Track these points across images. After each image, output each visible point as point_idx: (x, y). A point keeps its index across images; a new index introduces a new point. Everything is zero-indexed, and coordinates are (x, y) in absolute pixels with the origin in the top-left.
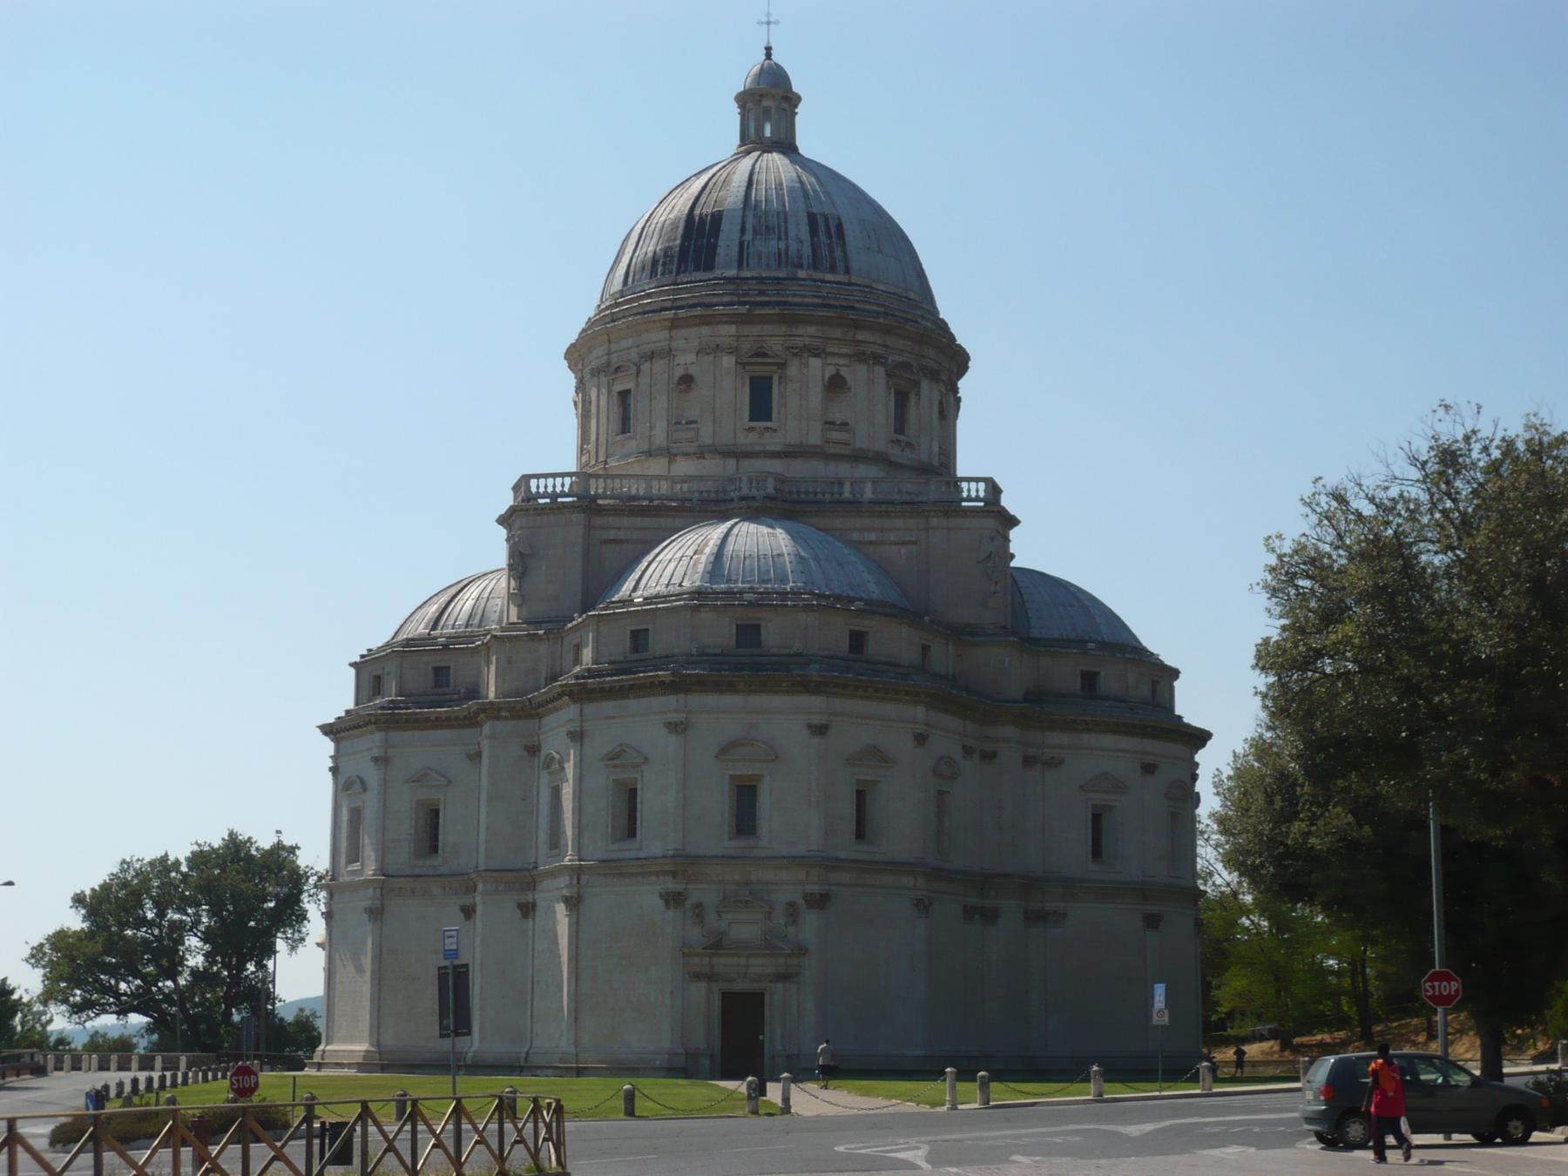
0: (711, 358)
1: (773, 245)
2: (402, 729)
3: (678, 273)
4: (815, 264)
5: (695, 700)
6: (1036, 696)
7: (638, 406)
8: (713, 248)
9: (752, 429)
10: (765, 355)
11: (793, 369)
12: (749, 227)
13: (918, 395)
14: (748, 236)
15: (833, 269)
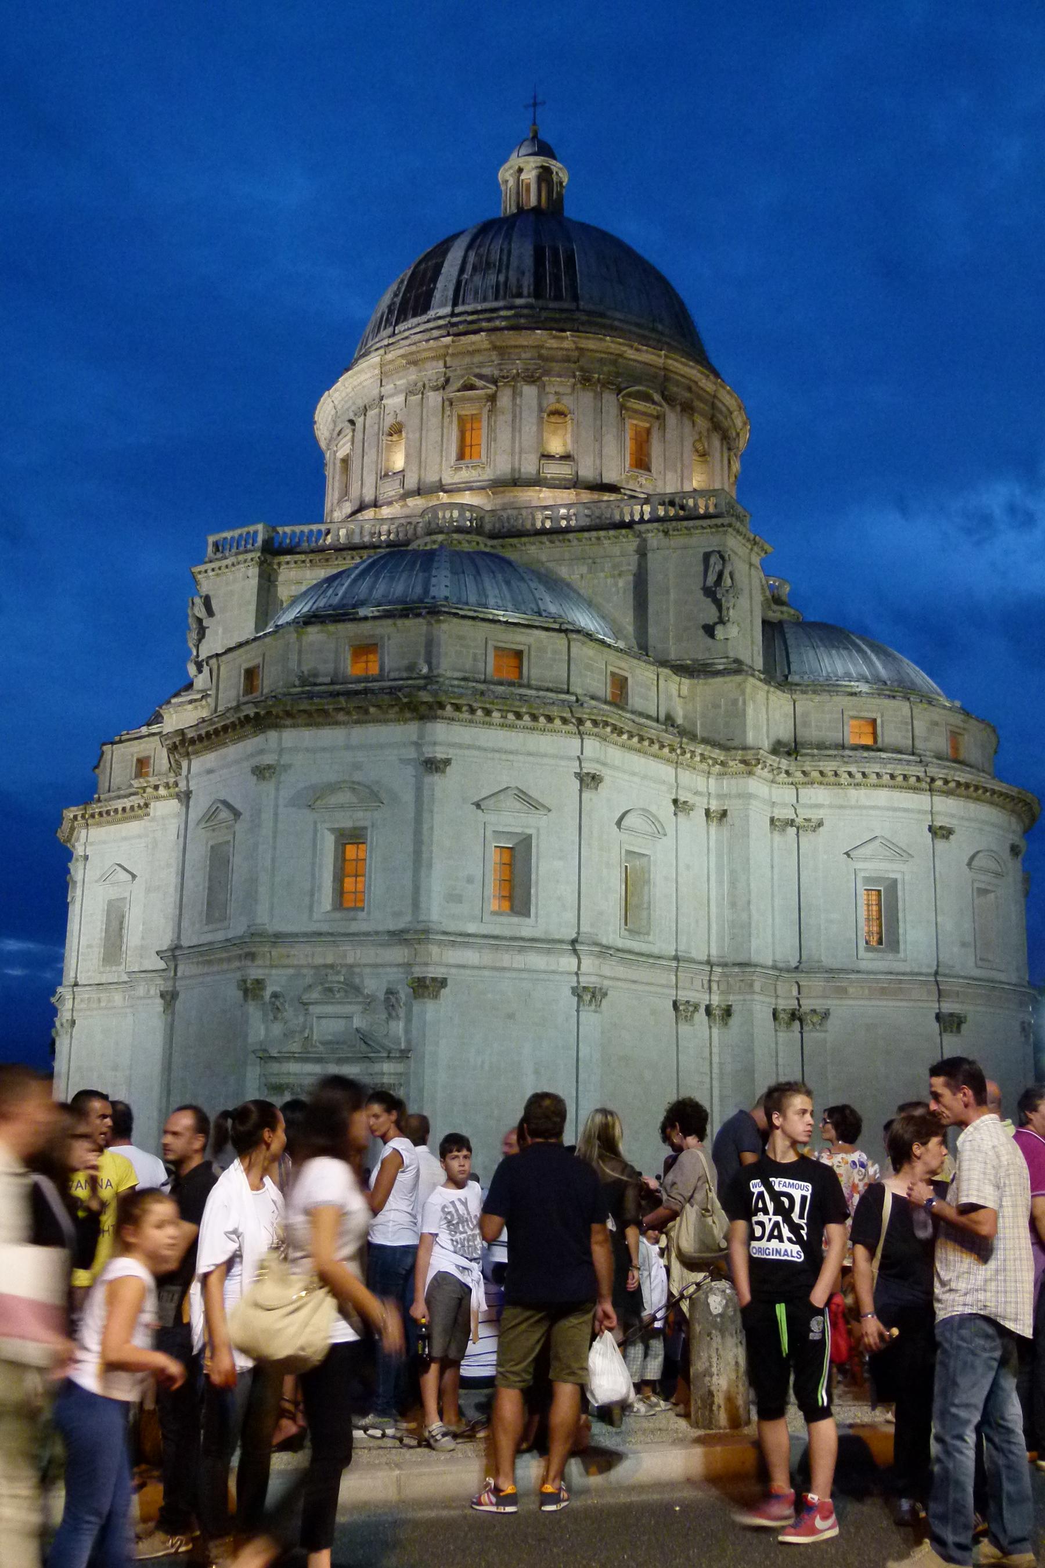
0: (415, 399)
1: (492, 278)
2: (99, 824)
3: (397, 324)
4: (538, 294)
5: (290, 737)
6: (790, 749)
7: (355, 466)
8: (429, 294)
9: (458, 469)
10: (472, 387)
11: (505, 399)
12: (469, 268)
13: (663, 428)
14: (465, 276)
15: (558, 297)
